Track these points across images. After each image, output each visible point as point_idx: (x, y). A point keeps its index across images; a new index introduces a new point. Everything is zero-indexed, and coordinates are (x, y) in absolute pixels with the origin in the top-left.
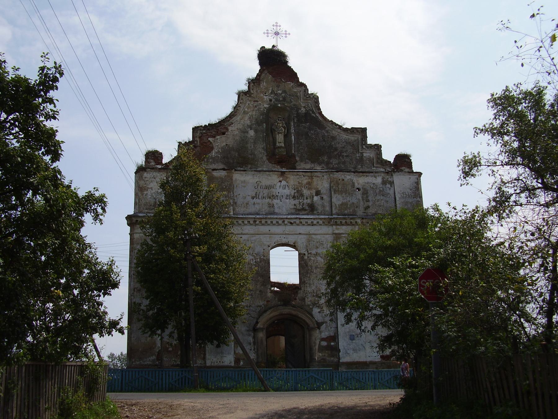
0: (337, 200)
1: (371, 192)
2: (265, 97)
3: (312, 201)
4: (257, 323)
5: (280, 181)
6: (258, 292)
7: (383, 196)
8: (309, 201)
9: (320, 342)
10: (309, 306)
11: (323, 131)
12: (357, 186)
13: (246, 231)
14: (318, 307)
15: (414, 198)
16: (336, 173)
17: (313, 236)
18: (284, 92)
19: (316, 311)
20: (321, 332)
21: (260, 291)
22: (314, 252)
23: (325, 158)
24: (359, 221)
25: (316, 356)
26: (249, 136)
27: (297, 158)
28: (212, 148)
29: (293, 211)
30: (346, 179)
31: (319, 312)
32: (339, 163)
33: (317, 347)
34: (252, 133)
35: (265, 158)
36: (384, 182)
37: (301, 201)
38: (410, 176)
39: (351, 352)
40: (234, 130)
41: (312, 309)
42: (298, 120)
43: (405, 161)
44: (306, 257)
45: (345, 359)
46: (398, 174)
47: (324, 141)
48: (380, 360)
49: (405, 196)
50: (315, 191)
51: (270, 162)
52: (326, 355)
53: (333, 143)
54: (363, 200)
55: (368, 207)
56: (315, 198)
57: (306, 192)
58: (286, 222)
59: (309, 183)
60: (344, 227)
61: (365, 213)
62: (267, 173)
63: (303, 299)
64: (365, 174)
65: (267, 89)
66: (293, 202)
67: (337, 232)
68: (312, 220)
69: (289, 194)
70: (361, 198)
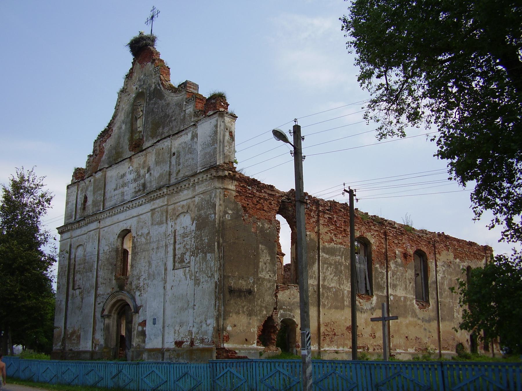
0: (157, 172)
1: (182, 154)
2: (134, 87)
3: (145, 180)
4: (103, 310)
5: (129, 168)
6: (108, 281)
7: (190, 153)
8: (142, 181)
9: (138, 327)
10: (134, 289)
11: (163, 101)
12: (173, 150)
13: (107, 224)
14: (139, 290)
15: (212, 146)
16: (158, 144)
17: (141, 216)
18: (145, 75)
19: (138, 293)
20: (139, 317)
21: (110, 279)
22: (140, 233)
23: (160, 130)
24: (165, 190)
25: (133, 341)
26: (122, 131)
27: (145, 139)
28: (104, 152)
29: (134, 194)
30: (164, 147)
31: (139, 296)
32: (169, 131)
33: (135, 332)
34: (124, 127)
35: (128, 148)
36: (193, 138)
37: (138, 182)
38: (211, 121)
39: (152, 337)
40: (115, 129)
41: (135, 292)
42: (149, 99)
43: (212, 103)
44: (135, 240)
45: (149, 345)
46: (201, 122)
47: (162, 111)
48: (174, 347)
49: (205, 146)
50: (147, 169)
51: (130, 151)
52: (141, 340)
53: (167, 111)
54: (176, 164)
55: (179, 171)
56: (147, 176)
57: (142, 172)
58: (125, 208)
59: (144, 162)
60: (158, 201)
61: (176, 179)
62: (123, 162)
63: (131, 284)
64: (179, 135)
65: (136, 79)
66: (135, 185)
67: (153, 207)
68: (139, 200)
69: (132, 178)
70: (175, 164)
